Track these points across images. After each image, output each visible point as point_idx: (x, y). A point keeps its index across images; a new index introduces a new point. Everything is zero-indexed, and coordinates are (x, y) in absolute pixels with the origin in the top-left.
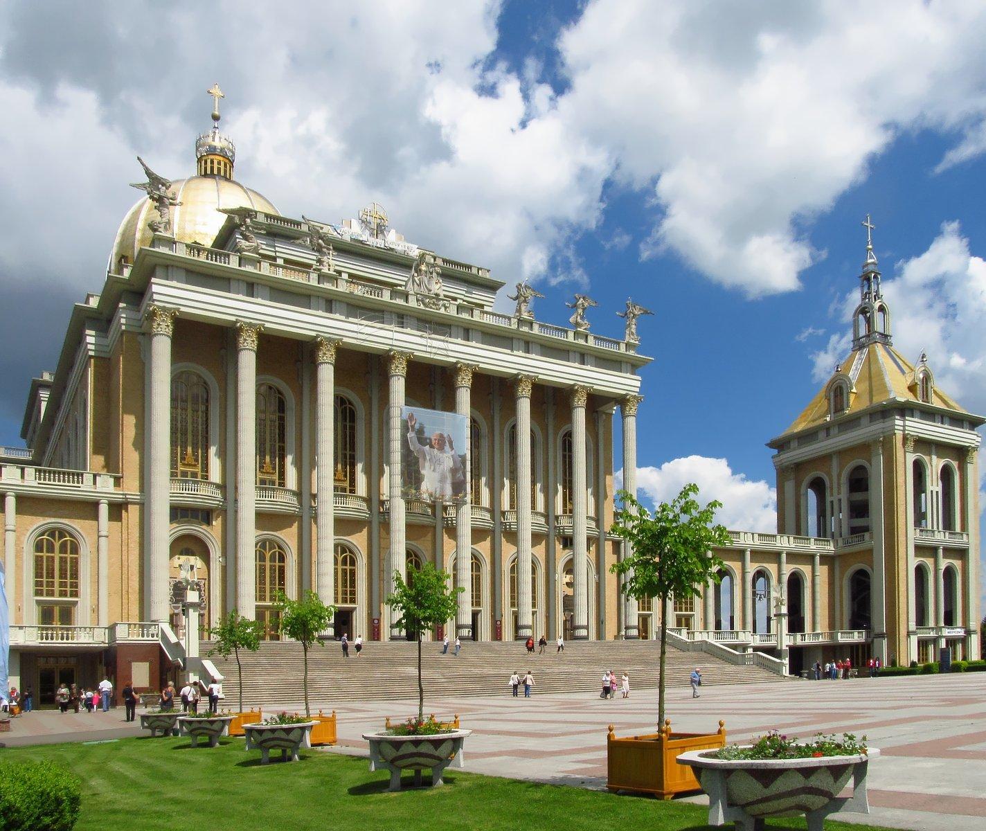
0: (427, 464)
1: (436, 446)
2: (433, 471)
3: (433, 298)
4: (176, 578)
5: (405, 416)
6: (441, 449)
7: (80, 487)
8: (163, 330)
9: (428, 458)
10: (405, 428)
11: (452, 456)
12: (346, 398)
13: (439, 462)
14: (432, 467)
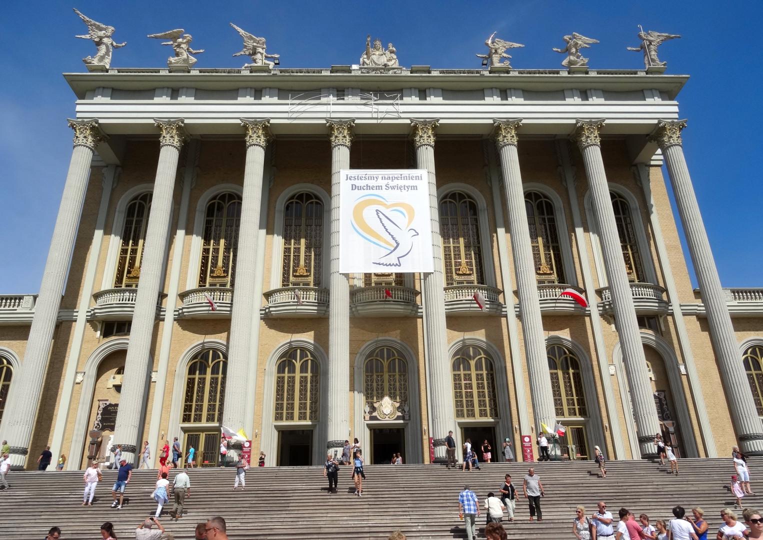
3: (382, 69)
4: (107, 400)
7: (16, 310)
8: (81, 141)
12: (312, 193)
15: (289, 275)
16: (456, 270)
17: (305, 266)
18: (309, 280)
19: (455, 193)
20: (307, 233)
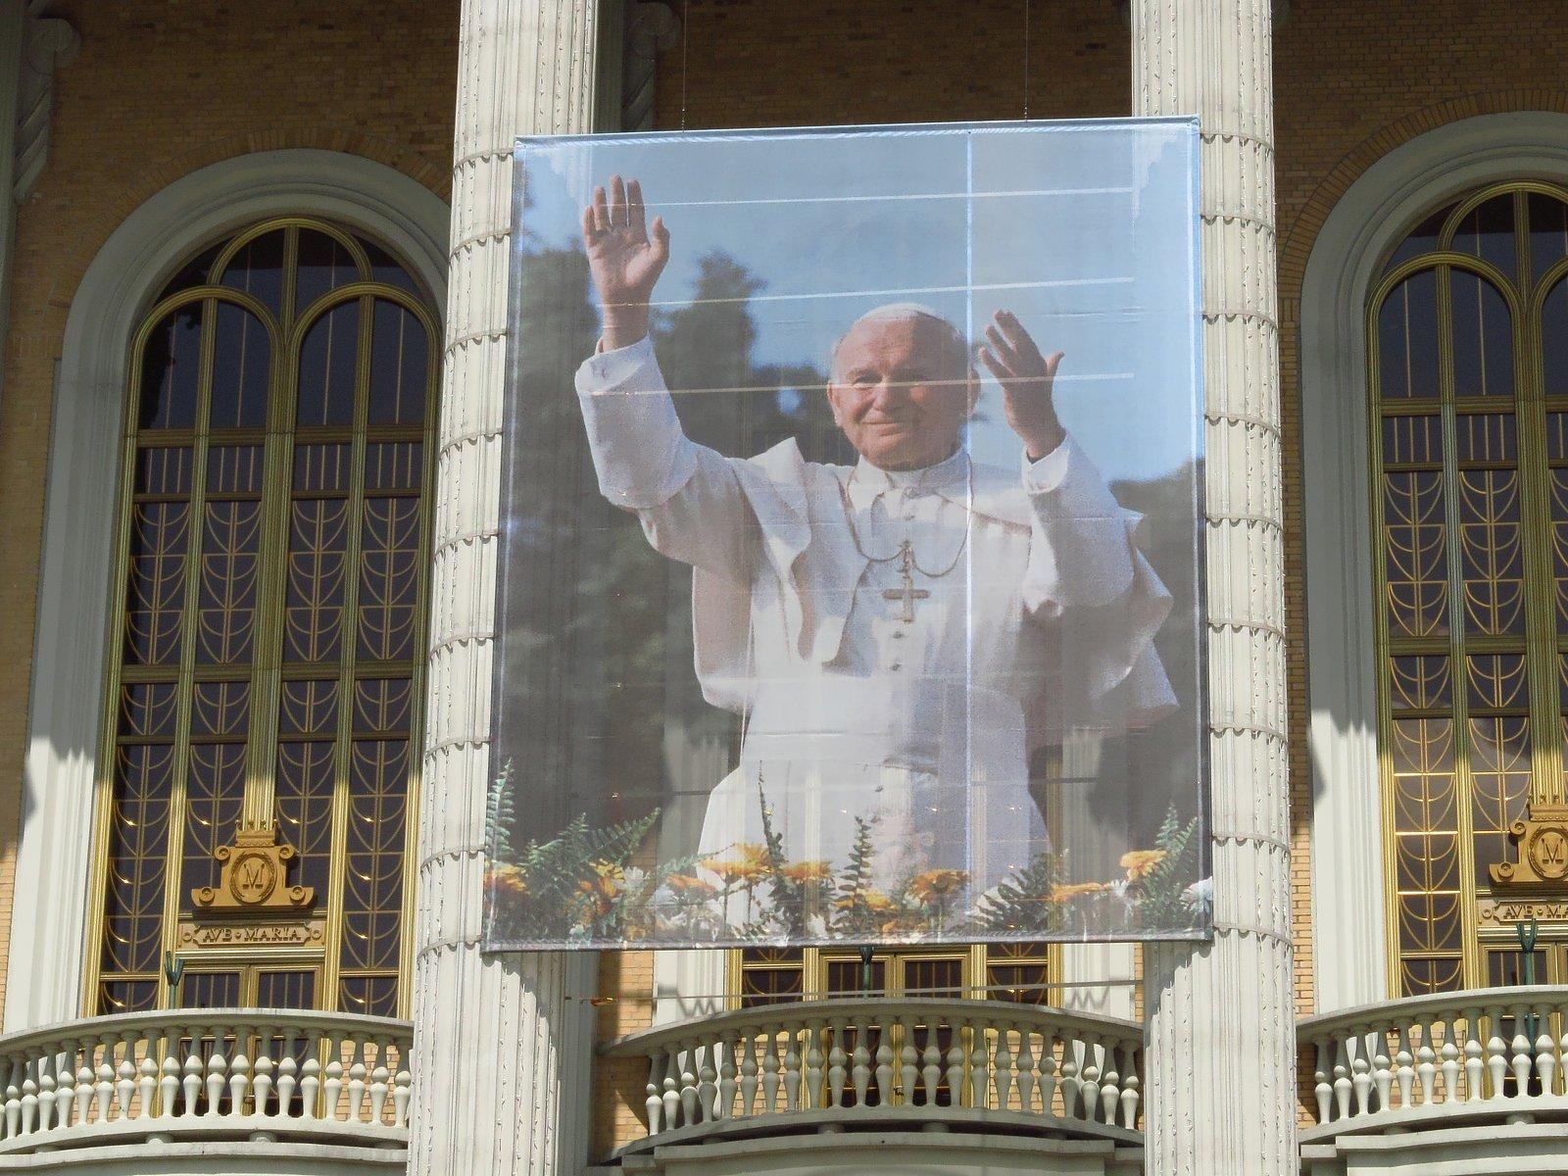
0: (775, 615)
1: (872, 437)
2: (842, 663)
5: (560, 223)
6: (925, 436)
9: (781, 552)
10: (556, 306)
11: (1048, 503)
13: (902, 572)
14: (828, 639)
15: (158, 906)
16: (1486, 852)
17: (283, 834)
18: (311, 949)
19: (1507, 200)
20: (306, 563)
